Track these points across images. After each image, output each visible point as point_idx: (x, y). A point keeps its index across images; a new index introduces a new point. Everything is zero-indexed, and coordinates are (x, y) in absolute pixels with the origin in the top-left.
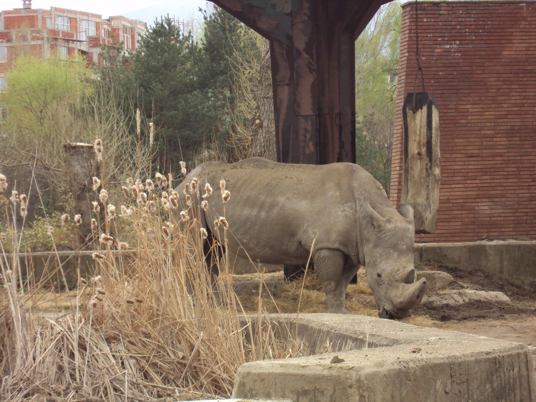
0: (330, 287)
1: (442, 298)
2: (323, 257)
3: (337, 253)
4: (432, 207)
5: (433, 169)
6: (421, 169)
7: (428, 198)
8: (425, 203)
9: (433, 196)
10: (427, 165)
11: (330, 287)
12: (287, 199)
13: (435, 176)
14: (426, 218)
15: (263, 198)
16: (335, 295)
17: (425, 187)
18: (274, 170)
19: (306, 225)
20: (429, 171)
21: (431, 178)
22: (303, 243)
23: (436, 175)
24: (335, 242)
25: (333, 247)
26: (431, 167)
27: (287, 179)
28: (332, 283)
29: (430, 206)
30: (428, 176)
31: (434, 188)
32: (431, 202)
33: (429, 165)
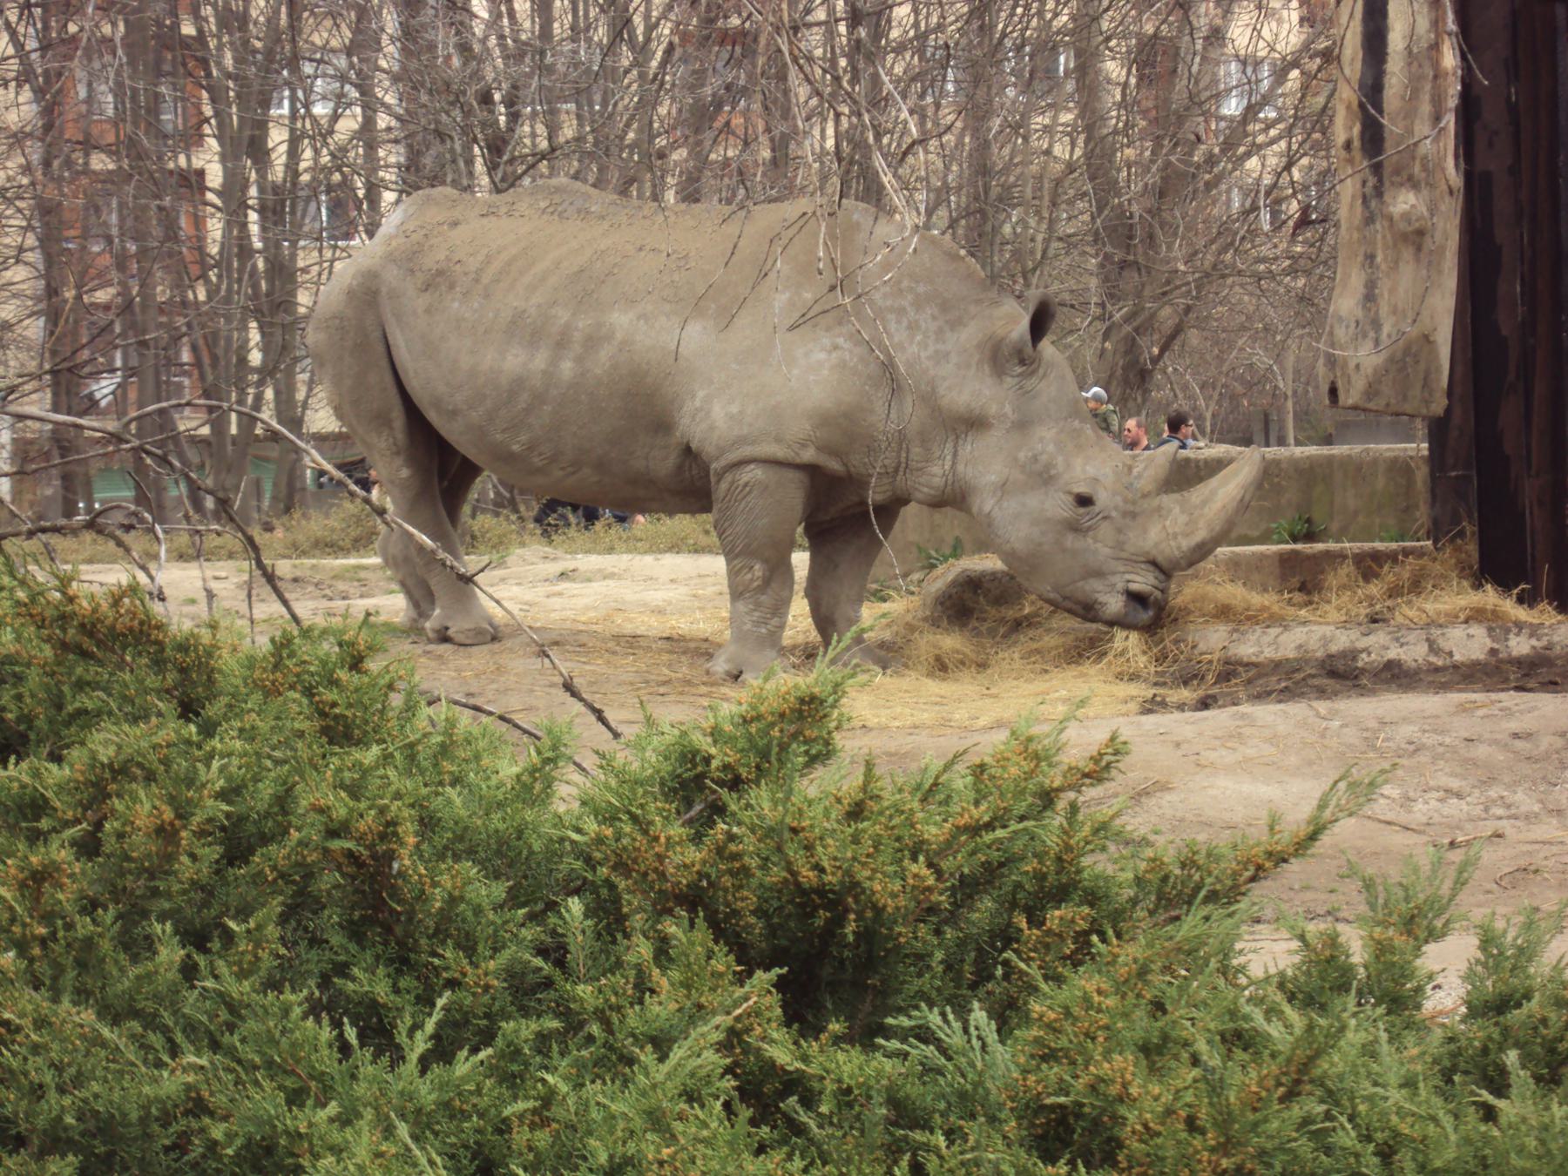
0: (749, 576)
1: (1397, 640)
2: (746, 485)
3: (791, 475)
4: (1386, 329)
5: (1387, 197)
6: (1353, 197)
7: (1370, 297)
8: (1360, 313)
9: (1392, 291)
10: (1364, 183)
11: (749, 576)
12: (638, 319)
13: (1391, 219)
14: (1358, 366)
15: (563, 315)
16: (758, 605)
17: (1360, 258)
18: (606, 225)
19: (701, 394)
20: (1373, 204)
21: (1378, 226)
22: (694, 446)
23: (1396, 217)
24: (804, 446)
25: (798, 461)
26: (1379, 192)
27: (643, 254)
28: (757, 567)
29: (1376, 324)
30: (1369, 220)
31: (1396, 262)
32: (1384, 310)
33: (1370, 184)
